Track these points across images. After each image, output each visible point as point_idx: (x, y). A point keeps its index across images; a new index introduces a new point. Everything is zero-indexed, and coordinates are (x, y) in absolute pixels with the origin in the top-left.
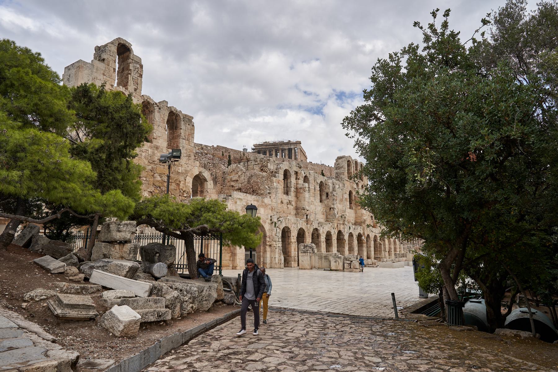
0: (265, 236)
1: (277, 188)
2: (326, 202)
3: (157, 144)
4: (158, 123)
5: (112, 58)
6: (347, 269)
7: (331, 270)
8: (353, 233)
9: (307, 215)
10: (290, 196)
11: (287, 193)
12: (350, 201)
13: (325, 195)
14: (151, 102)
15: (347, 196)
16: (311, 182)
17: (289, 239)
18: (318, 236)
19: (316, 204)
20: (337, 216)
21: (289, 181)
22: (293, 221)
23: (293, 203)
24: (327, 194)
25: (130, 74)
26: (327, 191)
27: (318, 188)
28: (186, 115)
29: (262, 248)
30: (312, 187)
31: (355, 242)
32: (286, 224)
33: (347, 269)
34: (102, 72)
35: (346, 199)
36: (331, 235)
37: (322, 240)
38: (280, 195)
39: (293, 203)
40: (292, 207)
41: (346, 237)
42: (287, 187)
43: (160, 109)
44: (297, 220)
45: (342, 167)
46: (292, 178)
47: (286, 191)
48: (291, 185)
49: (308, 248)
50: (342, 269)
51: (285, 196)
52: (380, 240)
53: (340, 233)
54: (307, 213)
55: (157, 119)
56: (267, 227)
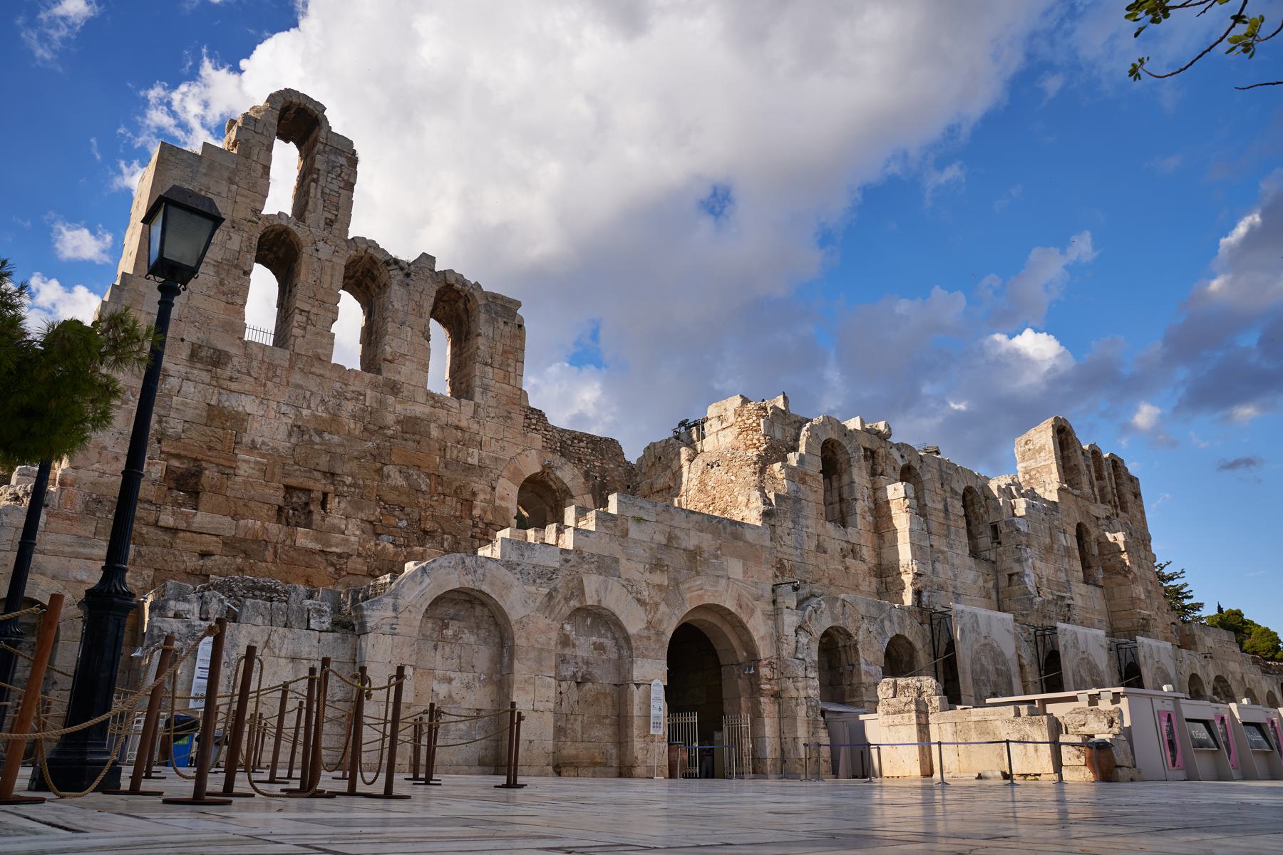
0: (754, 659)
3: (397, 378)
4: (400, 315)
5: (262, 139)
10: (849, 530)
11: (842, 518)
12: (1083, 560)
13: (989, 533)
14: (380, 256)
15: (1069, 540)
16: (928, 485)
19: (957, 561)
21: (845, 479)
22: (862, 609)
23: (867, 553)
24: (995, 528)
25: (316, 181)
26: (992, 518)
27: (957, 507)
28: (495, 297)
29: (744, 702)
32: (834, 620)
34: (226, 174)
38: (810, 522)
39: (867, 553)
40: (864, 567)
42: (841, 500)
43: (408, 275)
45: (1042, 449)
46: (855, 471)
47: (837, 515)
48: (852, 491)
51: (830, 526)
55: (397, 305)
56: (758, 627)
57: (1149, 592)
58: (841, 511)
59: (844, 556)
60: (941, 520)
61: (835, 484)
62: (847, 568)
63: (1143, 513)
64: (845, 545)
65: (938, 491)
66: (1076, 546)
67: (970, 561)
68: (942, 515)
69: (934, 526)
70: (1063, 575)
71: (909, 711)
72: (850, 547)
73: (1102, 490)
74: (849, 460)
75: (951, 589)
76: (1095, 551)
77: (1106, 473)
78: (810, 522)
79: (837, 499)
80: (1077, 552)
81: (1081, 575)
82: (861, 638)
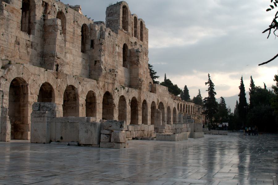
1: (8, 20)
2: (90, 53)
6: (105, 143)
7: (79, 145)
8: (126, 96)
9: (57, 66)
10: (31, 36)
15: (119, 50)
17: (24, 98)
18: (76, 97)
20: (104, 72)
21: (32, 14)
24: (92, 42)
27: (79, 32)
30: (69, 28)
31: (129, 108)
33: (105, 143)
35: (119, 53)
36: (94, 97)
37: (80, 103)
38: (14, 30)
41: (116, 101)
42: (30, 22)
44: (40, 71)
47: (27, 29)
49: (45, 109)
50: (95, 142)
52: (159, 108)
53: (108, 96)
54: (58, 61)
57: (144, 71)
58: (29, 27)
59: (28, 47)
60: (71, 36)
61: (28, 15)
62: (28, 52)
63: (147, 42)
64: (28, 42)
65: (72, 24)
66: (122, 52)
67: (81, 54)
68: (72, 34)
69: (68, 38)
70: (116, 63)
71: (44, 117)
72: (30, 43)
73: (135, 32)
74: (35, 5)
75: (72, 65)
76: (128, 54)
77: (138, 26)
78: (14, 30)
79: (27, 21)
80: (122, 55)
81: (122, 63)
82: (30, 83)
